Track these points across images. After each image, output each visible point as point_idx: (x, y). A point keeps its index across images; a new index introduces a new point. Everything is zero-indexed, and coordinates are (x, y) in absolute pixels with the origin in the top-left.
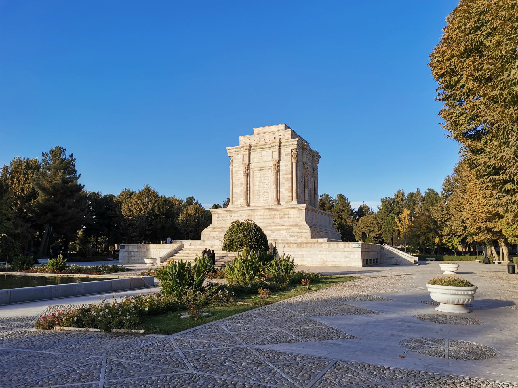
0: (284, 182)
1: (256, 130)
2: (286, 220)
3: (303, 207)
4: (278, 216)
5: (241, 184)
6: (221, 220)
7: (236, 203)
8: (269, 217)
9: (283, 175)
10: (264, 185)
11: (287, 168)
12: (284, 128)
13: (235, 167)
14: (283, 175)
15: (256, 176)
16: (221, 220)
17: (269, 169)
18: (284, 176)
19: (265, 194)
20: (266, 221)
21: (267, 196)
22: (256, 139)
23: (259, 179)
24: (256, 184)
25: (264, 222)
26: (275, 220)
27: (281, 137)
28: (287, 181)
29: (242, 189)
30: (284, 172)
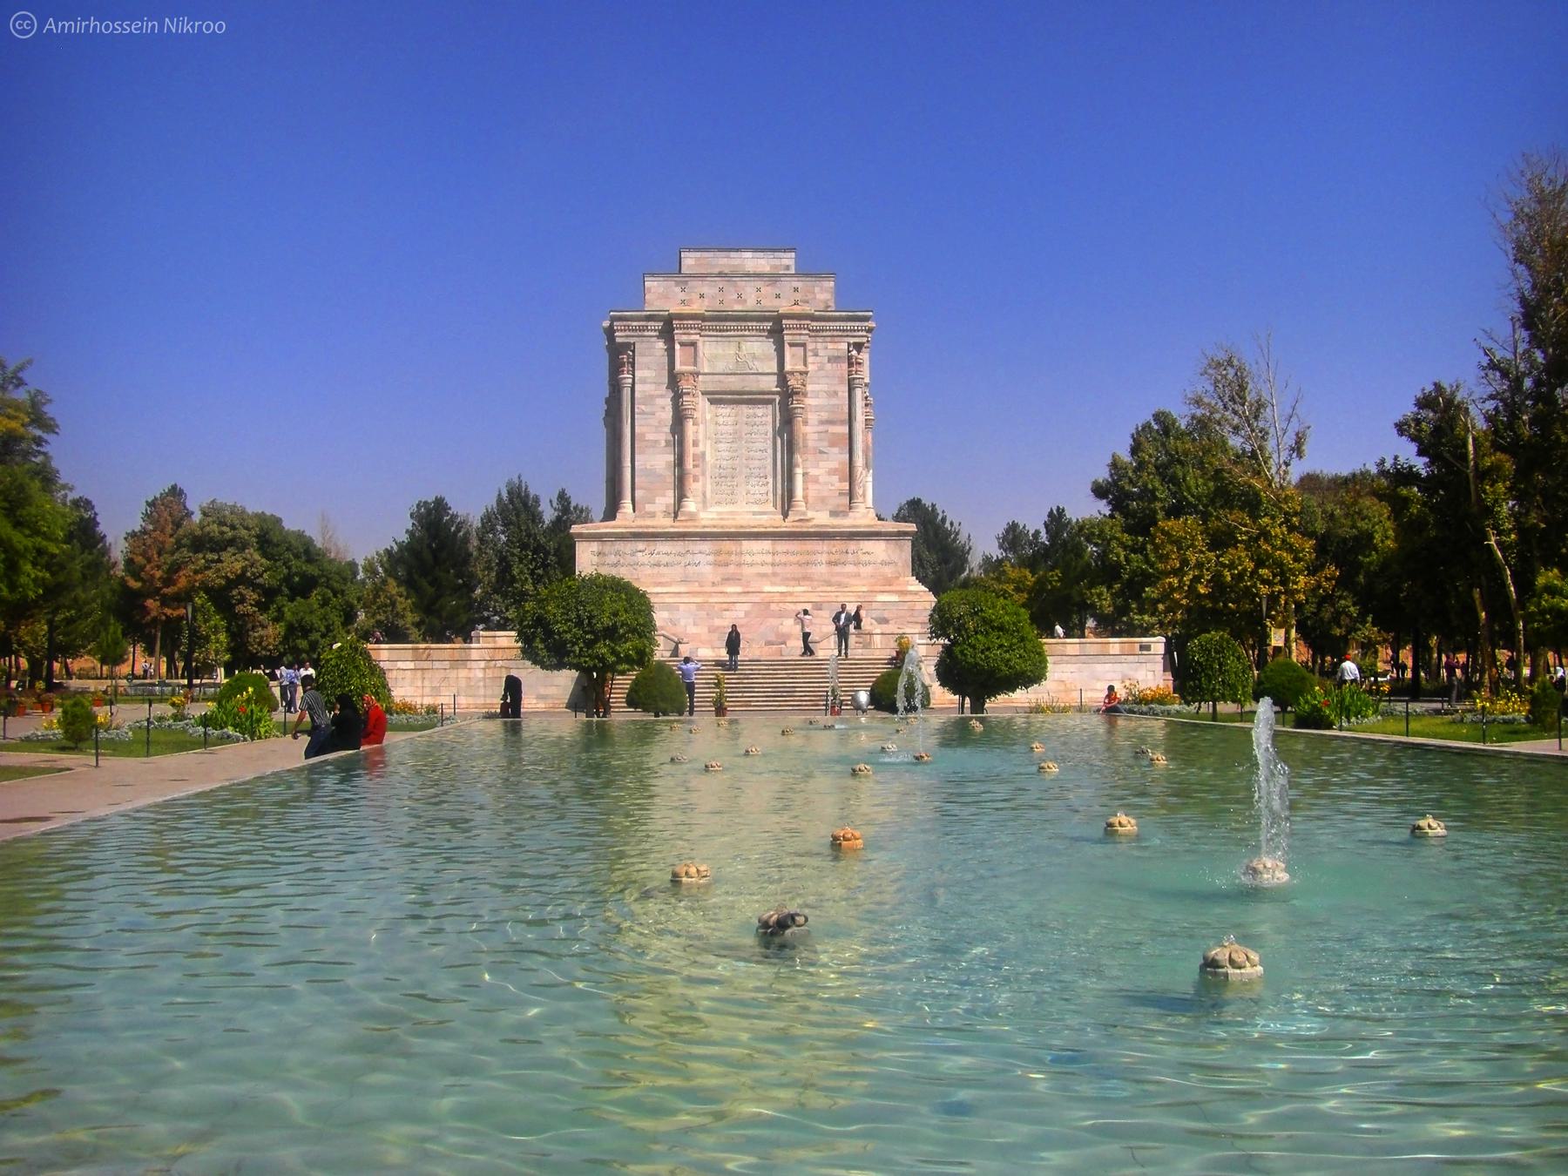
0: (823, 446)
1: (690, 260)
2: (850, 569)
3: (906, 534)
4: (824, 558)
6: (615, 565)
7: (649, 508)
9: (822, 423)
11: (834, 401)
12: (792, 263)
13: (644, 381)
14: (822, 423)
15: (721, 420)
16: (615, 565)
17: (771, 402)
18: (822, 428)
19: (753, 481)
20: (778, 569)
22: (706, 290)
23: (730, 429)
25: (775, 574)
26: (813, 570)
27: (798, 296)
28: (832, 445)
30: (825, 415)
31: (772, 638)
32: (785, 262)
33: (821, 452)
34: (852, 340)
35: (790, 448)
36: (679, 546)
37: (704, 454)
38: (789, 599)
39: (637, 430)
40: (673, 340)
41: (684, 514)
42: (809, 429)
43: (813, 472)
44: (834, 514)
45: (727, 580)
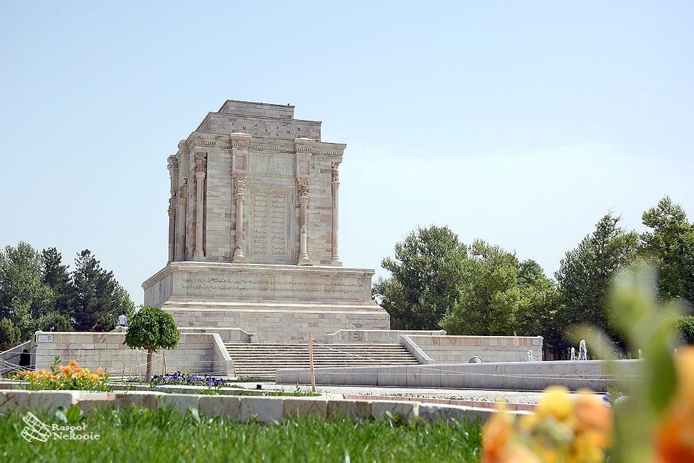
0: (317, 221)
5: (228, 215)
6: (199, 288)
8: (305, 288)
10: (274, 222)
11: (324, 196)
14: (316, 208)
15: (257, 203)
16: (199, 288)
21: (282, 246)
22: (247, 125)
23: (263, 209)
24: (256, 219)
26: (315, 294)
28: (322, 221)
29: (229, 224)
30: (319, 204)
31: (295, 334)
32: (289, 114)
33: (316, 225)
34: (334, 161)
35: (300, 221)
36: (238, 278)
37: (247, 223)
38: (305, 312)
39: (208, 206)
40: (231, 153)
41: (238, 258)
42: (310, 213)
43: (312, 237)
44: (323, 262)
45: (266, 298)
